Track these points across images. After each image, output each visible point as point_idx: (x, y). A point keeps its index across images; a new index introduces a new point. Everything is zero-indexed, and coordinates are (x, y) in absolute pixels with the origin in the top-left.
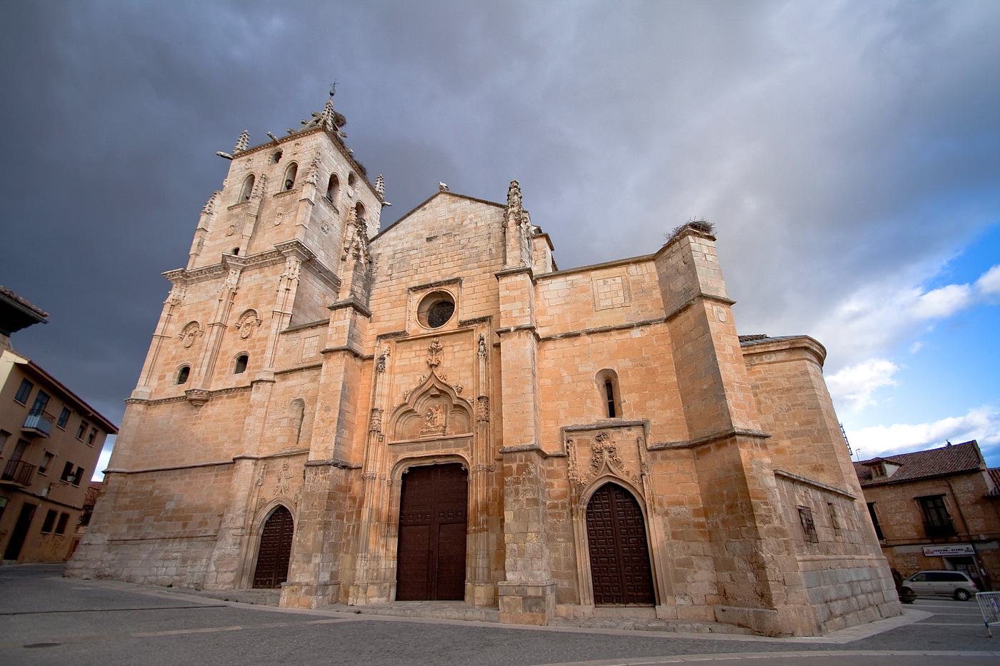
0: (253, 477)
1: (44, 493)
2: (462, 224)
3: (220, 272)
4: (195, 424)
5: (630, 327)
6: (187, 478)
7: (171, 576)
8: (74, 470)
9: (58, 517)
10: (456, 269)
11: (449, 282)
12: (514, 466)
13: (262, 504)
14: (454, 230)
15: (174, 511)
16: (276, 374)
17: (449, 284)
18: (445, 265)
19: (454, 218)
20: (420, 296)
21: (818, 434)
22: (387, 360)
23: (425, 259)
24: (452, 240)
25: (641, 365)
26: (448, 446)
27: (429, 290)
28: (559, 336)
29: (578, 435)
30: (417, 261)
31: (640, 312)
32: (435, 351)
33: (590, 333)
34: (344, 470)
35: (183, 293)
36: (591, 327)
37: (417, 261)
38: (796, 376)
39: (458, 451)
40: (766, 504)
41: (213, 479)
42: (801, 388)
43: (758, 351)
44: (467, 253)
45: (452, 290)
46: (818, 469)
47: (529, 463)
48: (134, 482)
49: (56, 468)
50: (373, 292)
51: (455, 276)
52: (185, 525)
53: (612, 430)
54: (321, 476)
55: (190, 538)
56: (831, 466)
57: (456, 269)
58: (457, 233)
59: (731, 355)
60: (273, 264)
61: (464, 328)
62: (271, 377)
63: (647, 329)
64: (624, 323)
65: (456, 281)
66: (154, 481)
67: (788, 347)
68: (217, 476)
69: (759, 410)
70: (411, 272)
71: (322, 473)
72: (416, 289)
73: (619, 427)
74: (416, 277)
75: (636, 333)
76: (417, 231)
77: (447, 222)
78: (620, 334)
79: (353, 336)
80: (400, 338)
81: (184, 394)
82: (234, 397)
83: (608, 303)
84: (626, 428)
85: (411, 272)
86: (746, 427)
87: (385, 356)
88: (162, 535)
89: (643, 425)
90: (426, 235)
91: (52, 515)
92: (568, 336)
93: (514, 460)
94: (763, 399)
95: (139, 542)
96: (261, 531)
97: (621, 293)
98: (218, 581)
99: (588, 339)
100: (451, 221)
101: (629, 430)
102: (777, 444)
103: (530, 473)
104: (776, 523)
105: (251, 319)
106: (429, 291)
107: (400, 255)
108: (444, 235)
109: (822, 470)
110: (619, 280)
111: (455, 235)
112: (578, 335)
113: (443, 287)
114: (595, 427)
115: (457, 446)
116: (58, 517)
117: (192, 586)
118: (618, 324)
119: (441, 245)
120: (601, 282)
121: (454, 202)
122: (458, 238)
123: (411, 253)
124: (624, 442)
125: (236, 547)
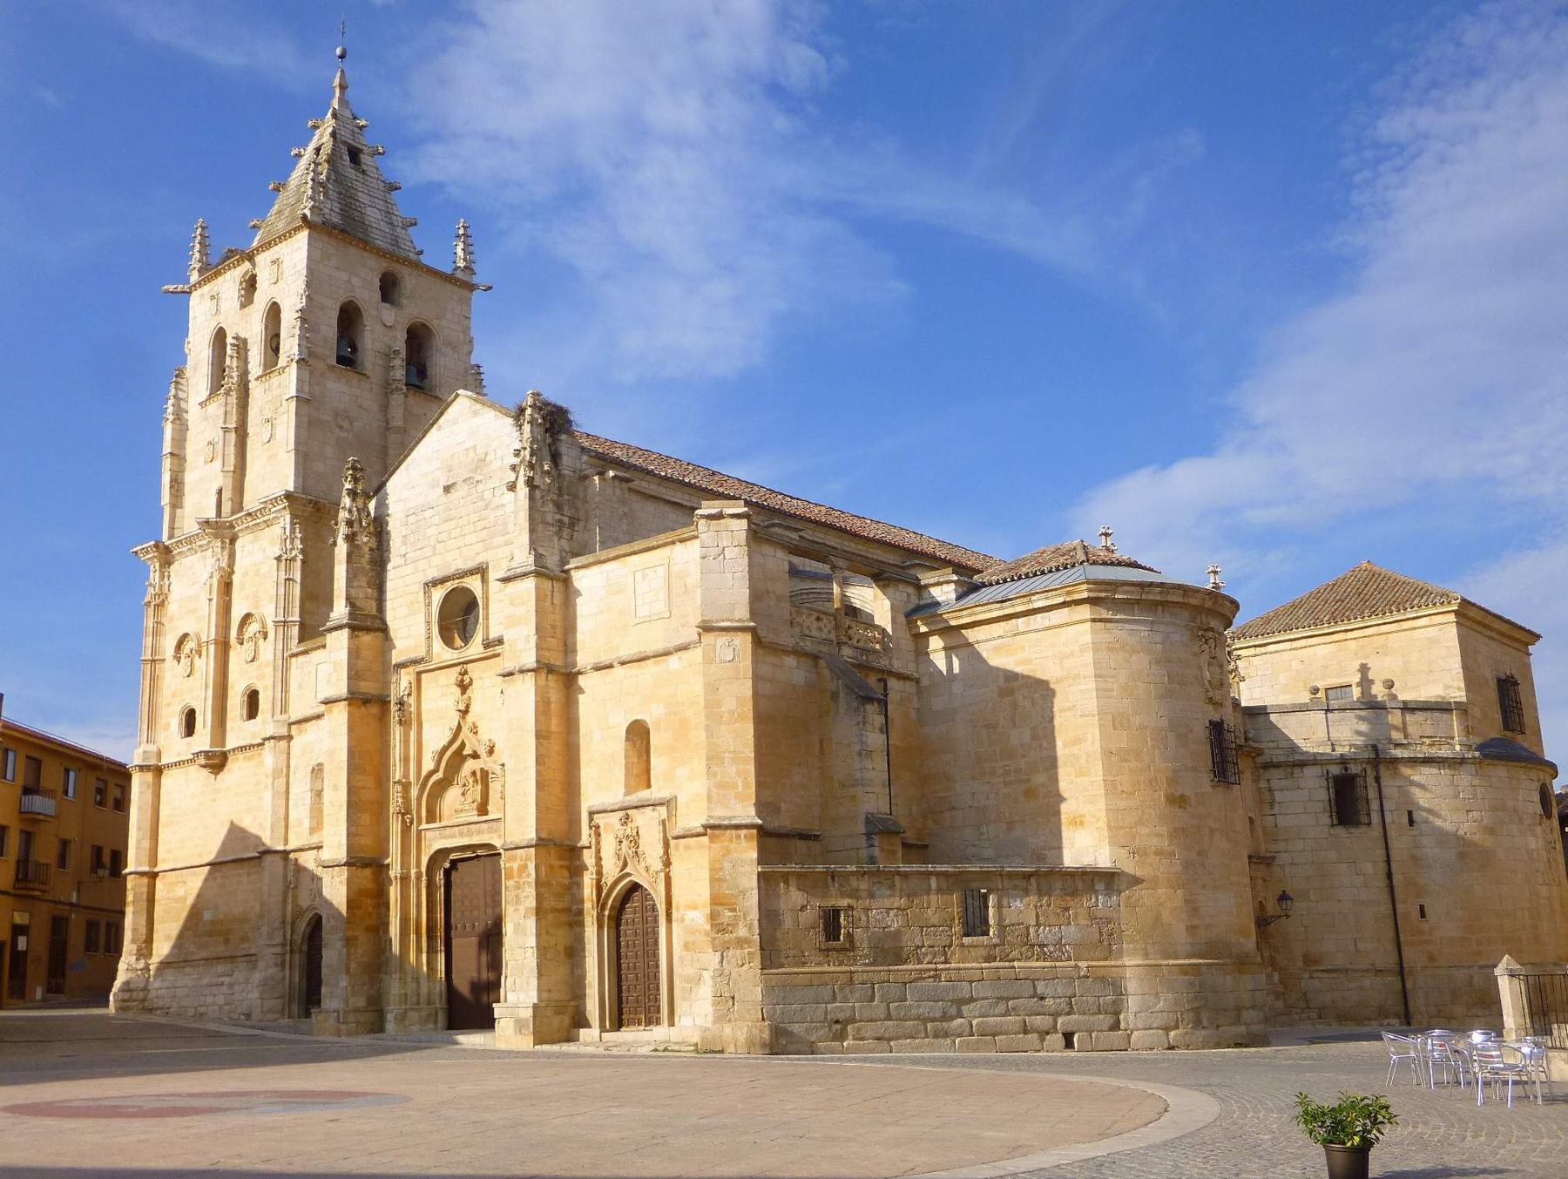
0: (285, 876)
1: (74, 899)
2: (484, 460)
3: (205, 542)
4: (214, 800)
5: (667, 654)
6: (219, 878)
7: (221, 1007)
8: (106, 858)
9: (103, 929)
10: (479, 547)
11: (471, 572)
12: (515, 866)
13: (298, 913)
14: (475, 470)
15: (213, 922)
16: (290, 725)
17: (472, 574)
18: (471, 539)
19: (475, 448)
20: (438, 594)
21: (1087, 761)
22: (412, 700)
23: (445, 526)
24: (473, 490)
25: (675, 715)
26: (479, 832)
27: (449, 584)
28: (589, 668)
29: (605, 818)
30: (432, 531)
31: (680, 628)
32: (464, 687)
33: (623, 663)
34: (367, 869)
35: (166, 579)
36: (625, 653)
37: (432, 531)
38: (1072, 654)
39: (492, 838)
40: (733, 910)
41: (245, 878)
42: (1076, 677)
43: (1019, 609)
44: (492, 517)
45: (474, 584)
46: (1076, 822)
47: (529, 863)
48: (164, 884)
49: (79, 856)
50: (389, 585)
51: (479, 560)
52: (227, 941)
53: (634, 810)
54: (338, 880)
55: (232, 958)
56: (1094, 817)
57: (479, 547)
58: (479, 478)
59: (732, 713)
60: (268, 526)
61: (491, 652)
62: (284, 731)
63: (683, 654)
64: (660, 646)
65: (481, 571)
66: (185, 882)
67: (1061, 600)
68: (249, 875)
69: (1014, 722)
70: (428, 551)
71: (338, 876)
72: (436, 583)
73: (643, 806)
74: (436, 560)
75: (674, 661)
76: (432, 472)
77: (467, 454)
78: (656, 663)
79: (356, 673)
80: (420, 668)
81: (192, 757)
82: (250, 759)
83: (643, 611)
84: (650, 808)
85: (428, 551)
86: (729, 814)
87: (405, 698)
88: (204, 954)
89: (669, 803)
90: (444, 483)
91: (92, 926)
92: (598, 668)
93: (514, 859)
94: (1020, 698)
95: (184, 964)
96: (305, 948)
97: (662, 595)
98: (264, 1009)
99: (618, 671)
100: (471, 454)
101: (654, 810)
102: (1028, 781)
103: (529, 875)
104: (742, 932)
105: (253, 628)
106: (450, 586)
107: (412, 519)
108: (464, 481)
109: (1082, 823)
110: (661, 571)
111: (477, 482)
112: (610, 666)
113: (465, 580)
114: (616, 807)
115: (490, 831)
116: (103, 929)
117: (242, 1017)
118: (653, 649)
119: (462, 501)
120: (639, 575)
121: (475, 413)
122: (480, 487)
123: (429, 513)
124: (648, 824)
125: (279, 969)
